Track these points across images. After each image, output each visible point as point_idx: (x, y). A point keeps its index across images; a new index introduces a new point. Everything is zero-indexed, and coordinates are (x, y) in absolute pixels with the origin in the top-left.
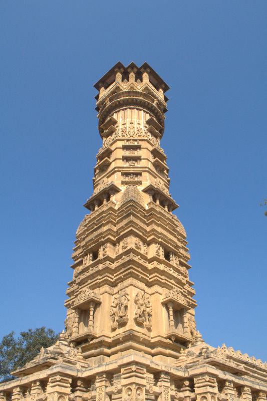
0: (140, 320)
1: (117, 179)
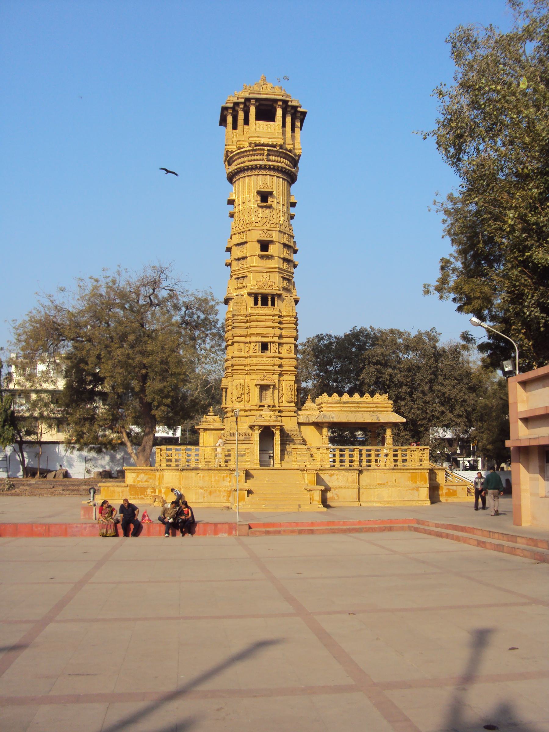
0: (239, 400)
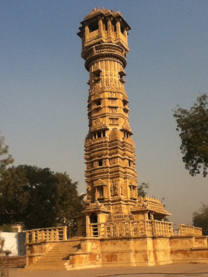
1: (106, 122)
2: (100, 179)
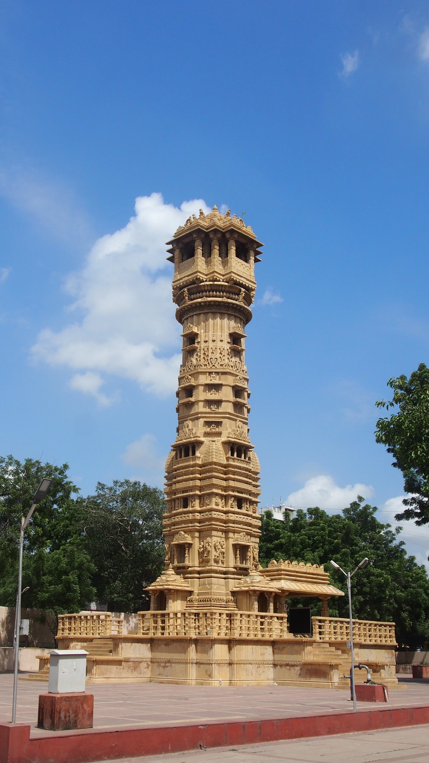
2: (183, 533)
